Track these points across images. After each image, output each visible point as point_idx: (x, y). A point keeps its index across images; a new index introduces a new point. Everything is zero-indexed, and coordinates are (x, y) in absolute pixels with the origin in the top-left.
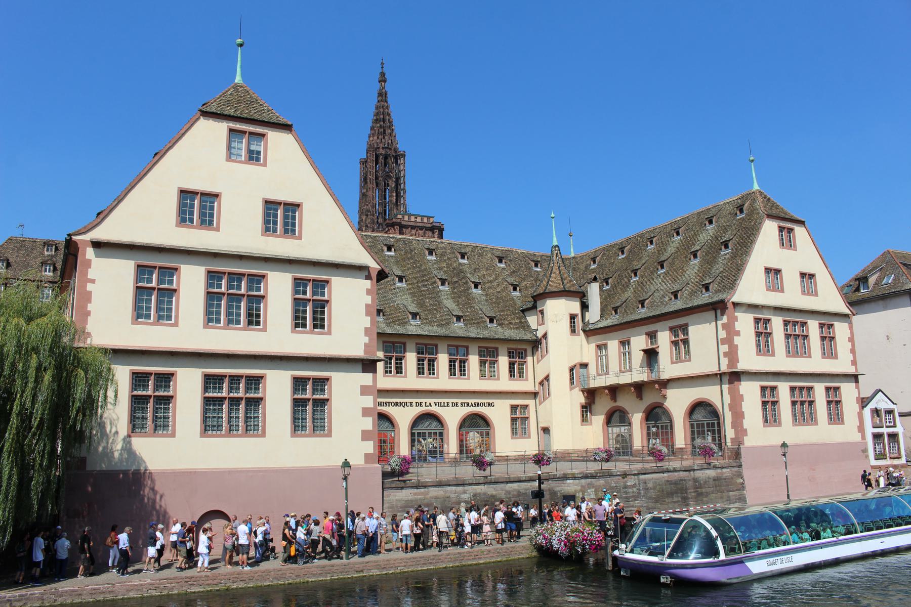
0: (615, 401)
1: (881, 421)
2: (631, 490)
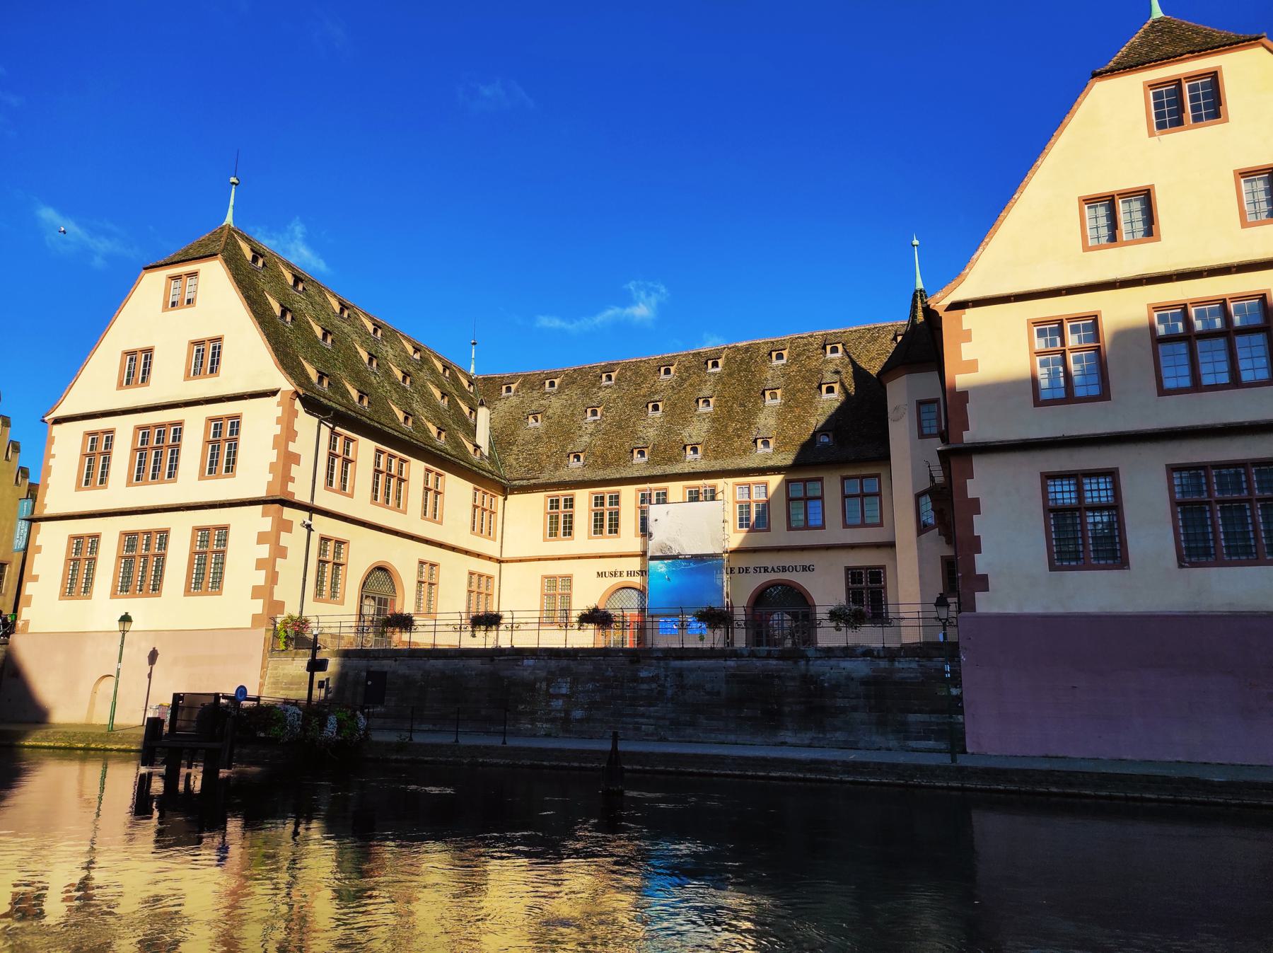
2: (645, 686)
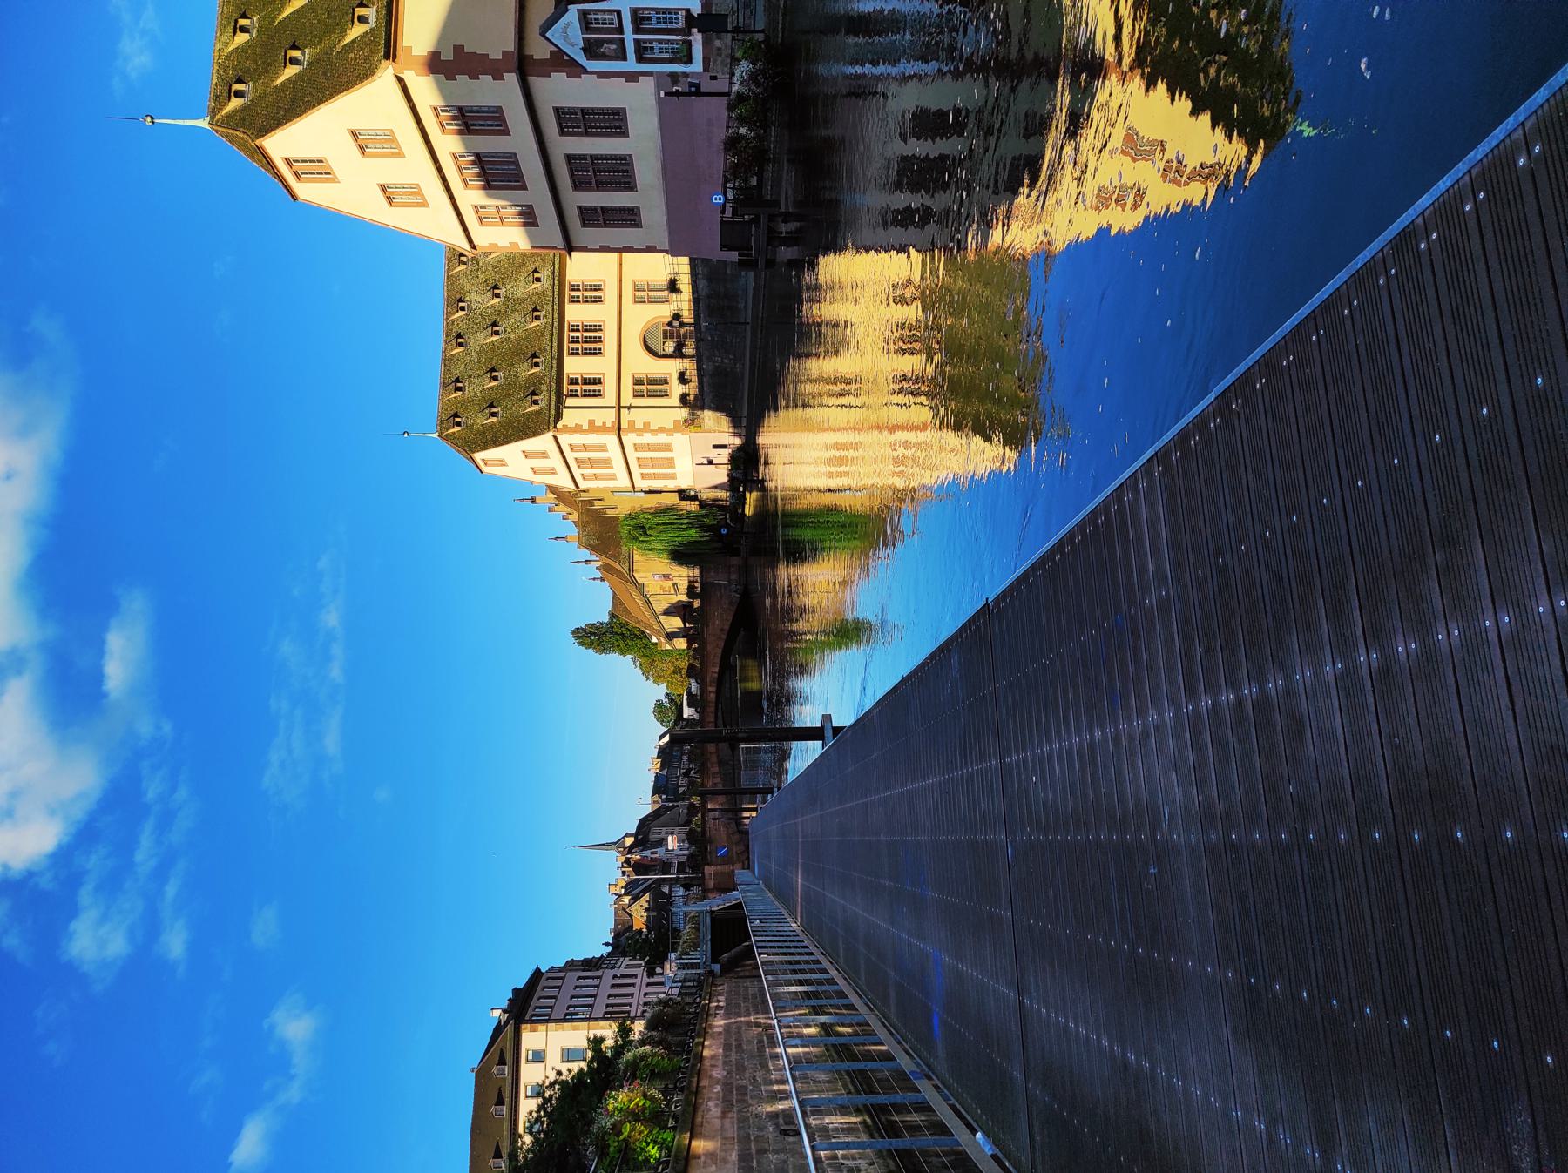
1: (610, 41)
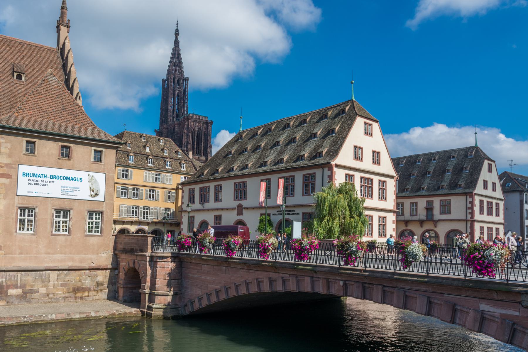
0: (407, 226)
